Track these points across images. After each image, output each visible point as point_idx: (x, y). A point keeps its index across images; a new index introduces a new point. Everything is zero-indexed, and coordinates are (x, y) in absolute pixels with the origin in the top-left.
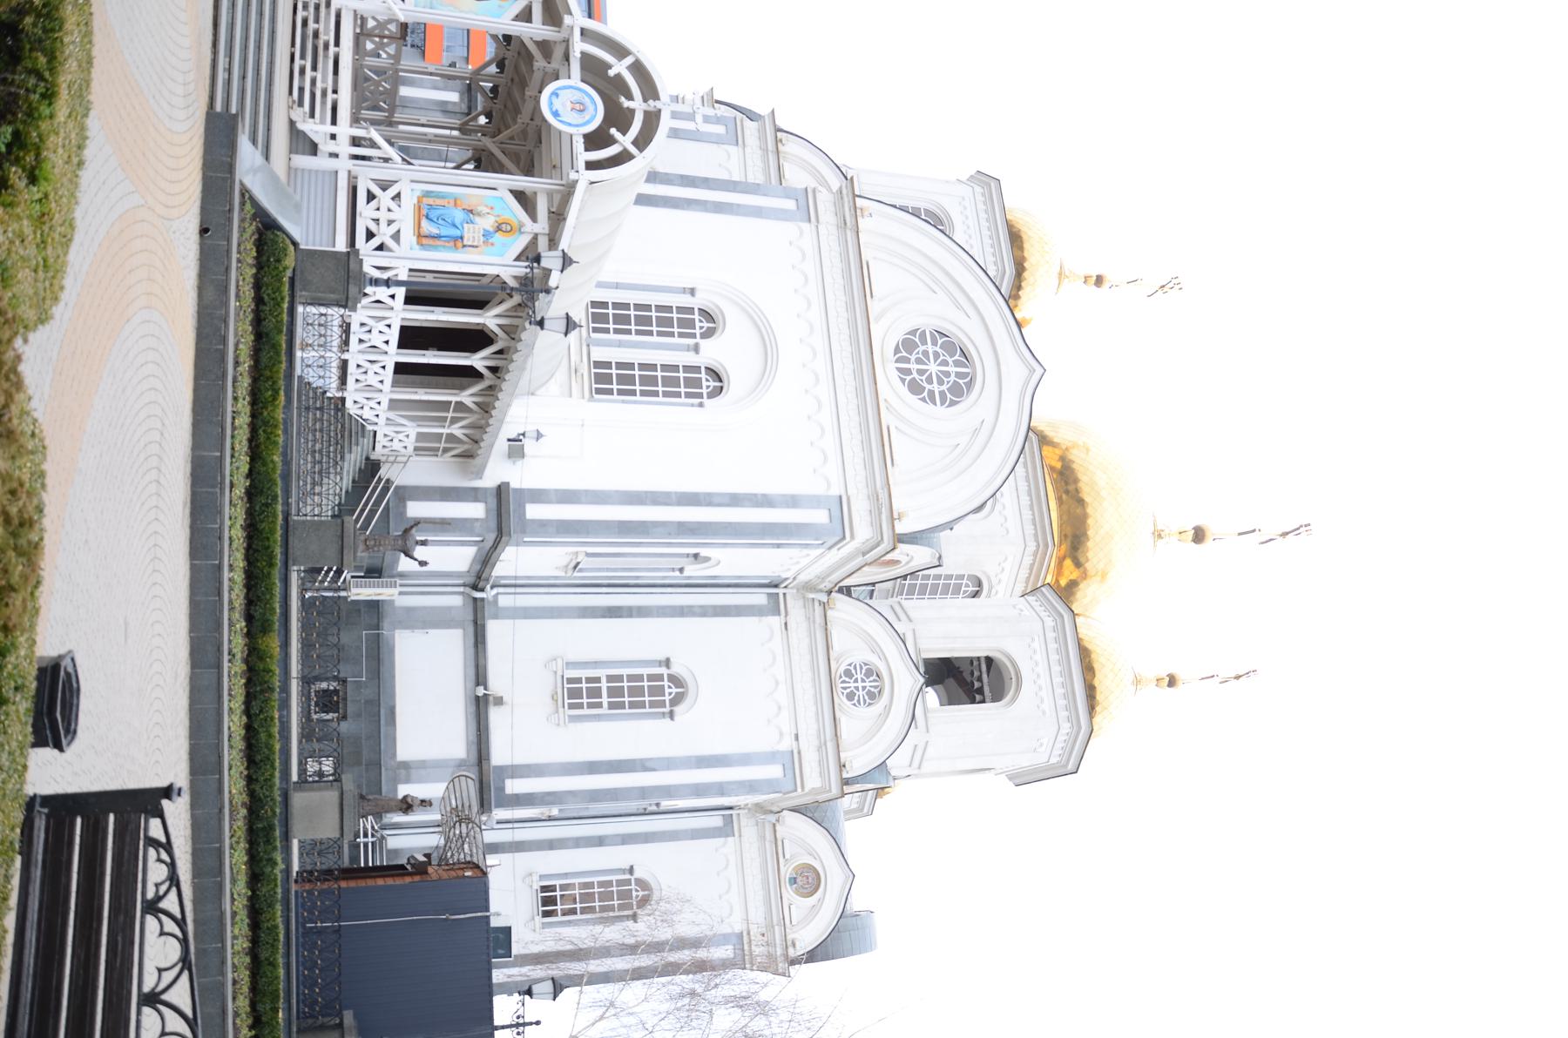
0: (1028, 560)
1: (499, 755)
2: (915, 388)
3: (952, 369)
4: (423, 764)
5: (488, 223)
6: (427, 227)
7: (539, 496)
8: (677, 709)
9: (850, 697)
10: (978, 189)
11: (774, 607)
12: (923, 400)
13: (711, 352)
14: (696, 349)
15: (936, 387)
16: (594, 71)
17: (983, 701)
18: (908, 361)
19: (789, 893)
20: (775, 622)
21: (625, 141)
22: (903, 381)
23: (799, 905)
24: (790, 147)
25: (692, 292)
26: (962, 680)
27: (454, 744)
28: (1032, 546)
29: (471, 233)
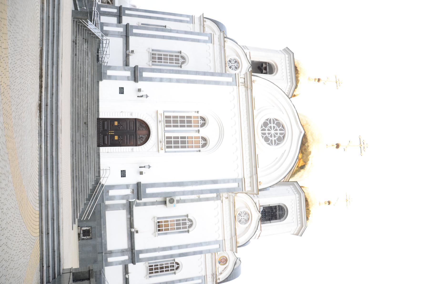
1: (138, 247)
2: (266, 139)
3: (278, 132)
8: (190, 229)
9: (240, 221)
10: (287, 56)
11: (218, 197)
12: (269, 144)
13: (204, 132)
17: (276, 219)
18: (265, 130)
19: (218, 264)
20: (219, 202)
22: (263, 137)
23: (221, 267)
24: (228, 43)
25: (198, 112)
26: (272, 214)
27: (124, 244)
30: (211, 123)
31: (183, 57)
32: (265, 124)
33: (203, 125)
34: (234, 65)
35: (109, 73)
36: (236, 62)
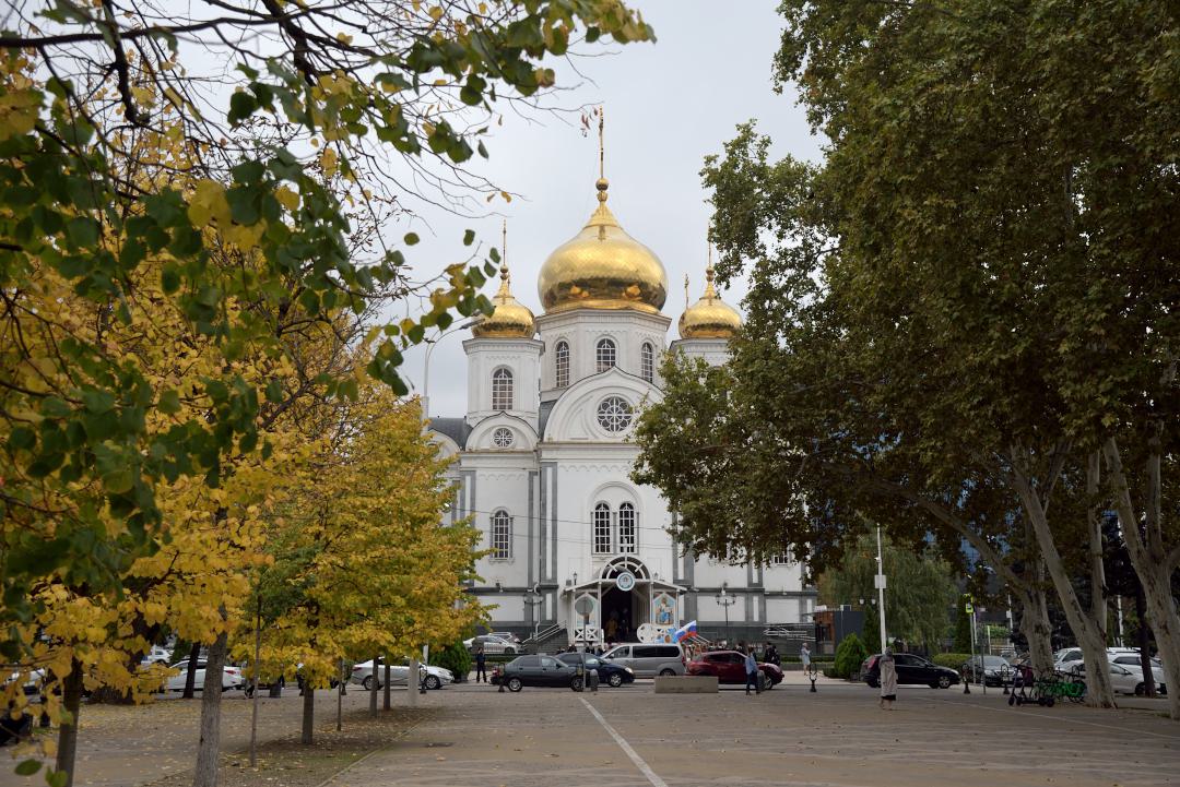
0: (638, 321)
4: (747, 612)
5: (664, 606)
6: (667, 622)
7: (675, 573)
10: (481, 348)
13: (615, 508)
14: (615, 514)
15: (623, 415)
16: (614, 575)
18: (612, 426)
21: (638, 568)
28: (632, 319)
29: (667, 610)
30: (604, 497)
31: (498, 514)
32: (605, 424)
33: (606, 507)
34: (503, 437)
35: (549, 617)
36: (499, 434)
